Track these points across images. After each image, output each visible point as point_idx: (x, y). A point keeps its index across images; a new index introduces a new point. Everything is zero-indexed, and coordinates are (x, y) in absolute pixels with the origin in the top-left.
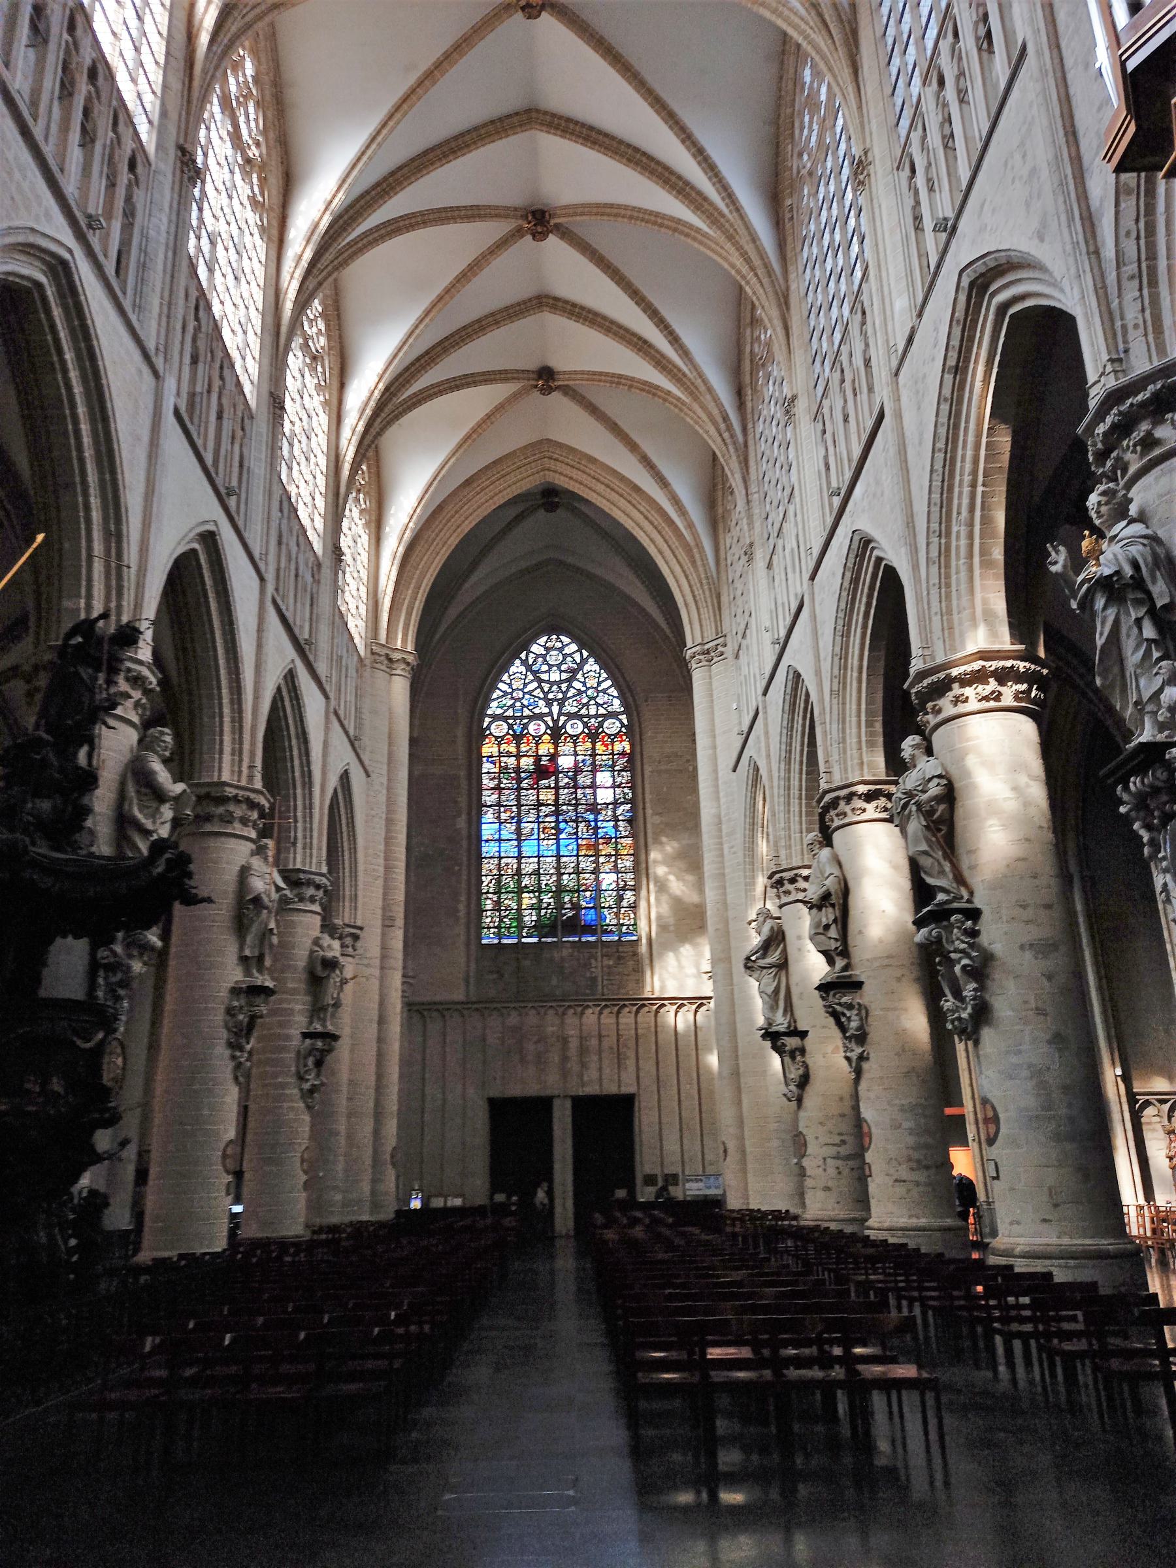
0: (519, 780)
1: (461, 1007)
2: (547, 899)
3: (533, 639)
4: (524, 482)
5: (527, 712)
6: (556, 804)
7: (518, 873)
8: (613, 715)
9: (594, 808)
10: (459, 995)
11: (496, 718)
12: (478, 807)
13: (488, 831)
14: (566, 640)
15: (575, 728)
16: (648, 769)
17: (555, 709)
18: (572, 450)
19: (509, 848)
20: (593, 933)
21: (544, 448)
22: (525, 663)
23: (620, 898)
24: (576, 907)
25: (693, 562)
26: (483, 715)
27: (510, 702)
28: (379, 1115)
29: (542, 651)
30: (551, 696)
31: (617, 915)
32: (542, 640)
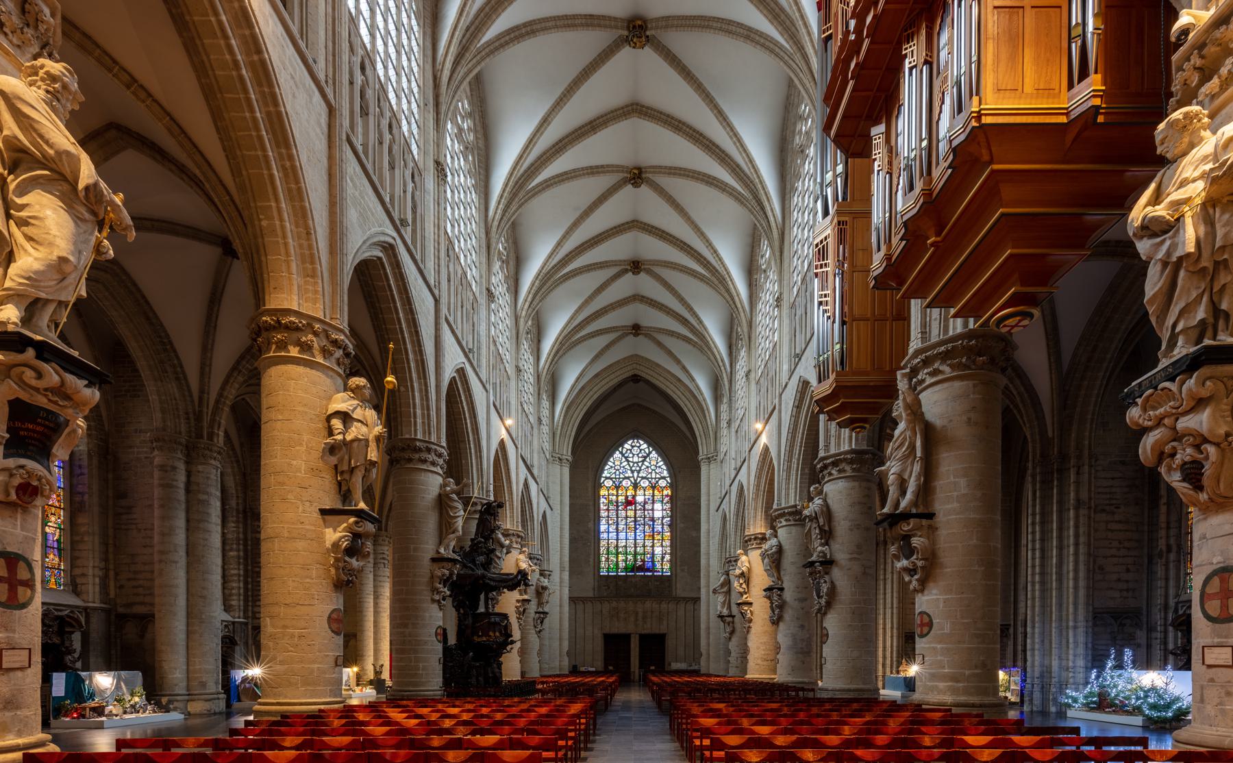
1: (591, 600)
2: (629, 557)
3: (626, 442)
4: (625, 374)
6: (635, 517)
7: (617, 546)
8: (664, 478)
9: (653, 519)
10: (591, 594)
11: (607, 478)
12: (597, 518)
13: (603, 528)
14: (642, 442)
15: (645, 483)
16: (679, 503)
17: (636, 474)
18: (647, 359)
19: (613, 535)
21: (635, 359)
22: (621, 453)
23: (663, 558)
24: (643, 561)
25: (705, 417)
26: (601, 477)
29: (630, 447)
32: (630, 442)
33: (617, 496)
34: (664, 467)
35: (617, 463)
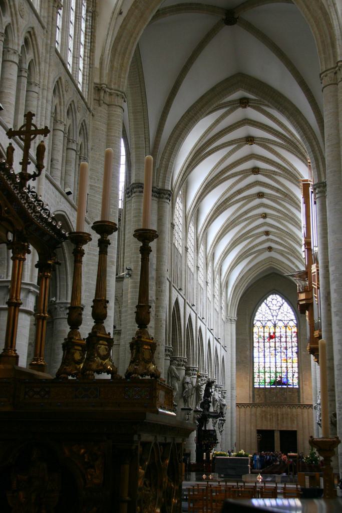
0: (264, 340)
2: (273, 375)
3: (268, 296)
5: (266, 319)
6: (275, 347)
8: (292, 320)
11: (257, 321)
13: (256, 354)
16: (302, 337)
17: (275, 317)
19: (262, 360)
20: (286, 385)
21: (271, 259)
22: (266, 304)
23: (293, 375)
26: (254, 320)
27: (262, 316)
28: (231, 435)
30: (273, 314)
31: (293, 380)
32: (271, 296)
33: (264, 333)
34: (292, 313)
35: (264, 310)
